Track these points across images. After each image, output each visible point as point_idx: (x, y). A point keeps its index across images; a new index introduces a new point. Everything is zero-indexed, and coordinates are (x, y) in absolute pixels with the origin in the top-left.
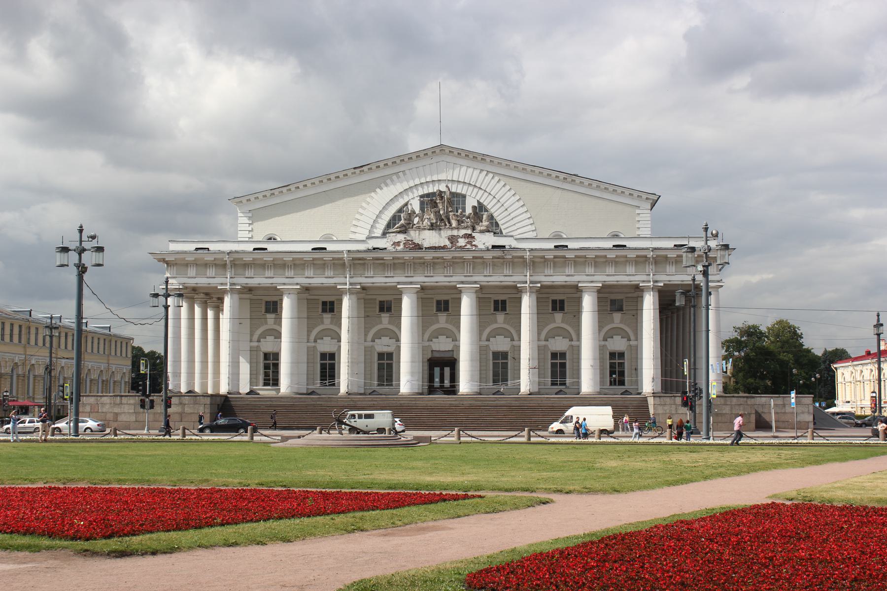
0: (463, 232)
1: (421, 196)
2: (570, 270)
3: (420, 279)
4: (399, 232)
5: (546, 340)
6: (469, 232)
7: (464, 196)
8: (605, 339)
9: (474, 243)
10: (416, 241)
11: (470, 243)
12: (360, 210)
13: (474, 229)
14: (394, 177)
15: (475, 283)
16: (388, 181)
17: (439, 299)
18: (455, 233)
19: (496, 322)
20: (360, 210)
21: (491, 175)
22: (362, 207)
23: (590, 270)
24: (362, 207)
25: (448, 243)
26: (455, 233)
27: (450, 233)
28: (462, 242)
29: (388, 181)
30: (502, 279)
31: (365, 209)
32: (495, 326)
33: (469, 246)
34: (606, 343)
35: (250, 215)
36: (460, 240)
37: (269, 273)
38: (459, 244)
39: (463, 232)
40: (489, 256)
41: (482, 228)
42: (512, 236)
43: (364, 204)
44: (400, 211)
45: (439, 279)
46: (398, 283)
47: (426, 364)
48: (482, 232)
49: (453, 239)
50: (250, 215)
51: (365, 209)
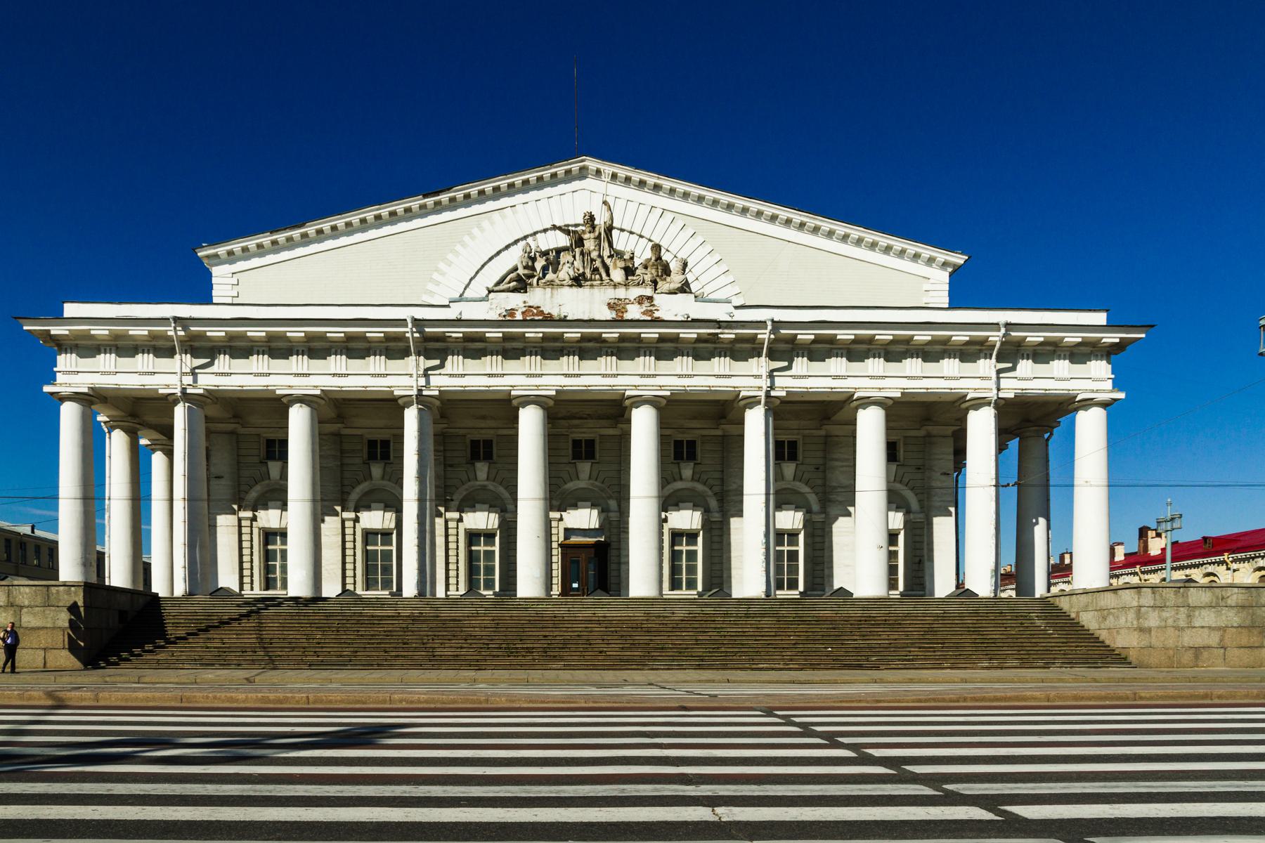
6: (648, 291)
9: (657, 314)
12: (436, 276)
15: (661, 387)
17: (577, 436)
18: (621, 293)
19: (681, 479)
20: (436, 276)
22: (437, 270)
24: (437, 270)
31: (443, 274)
32: (679, 485)
36: (628, 307)
38: (628, 316)
39: (635, 292)
40: (690, 334)
43: (442, 266)
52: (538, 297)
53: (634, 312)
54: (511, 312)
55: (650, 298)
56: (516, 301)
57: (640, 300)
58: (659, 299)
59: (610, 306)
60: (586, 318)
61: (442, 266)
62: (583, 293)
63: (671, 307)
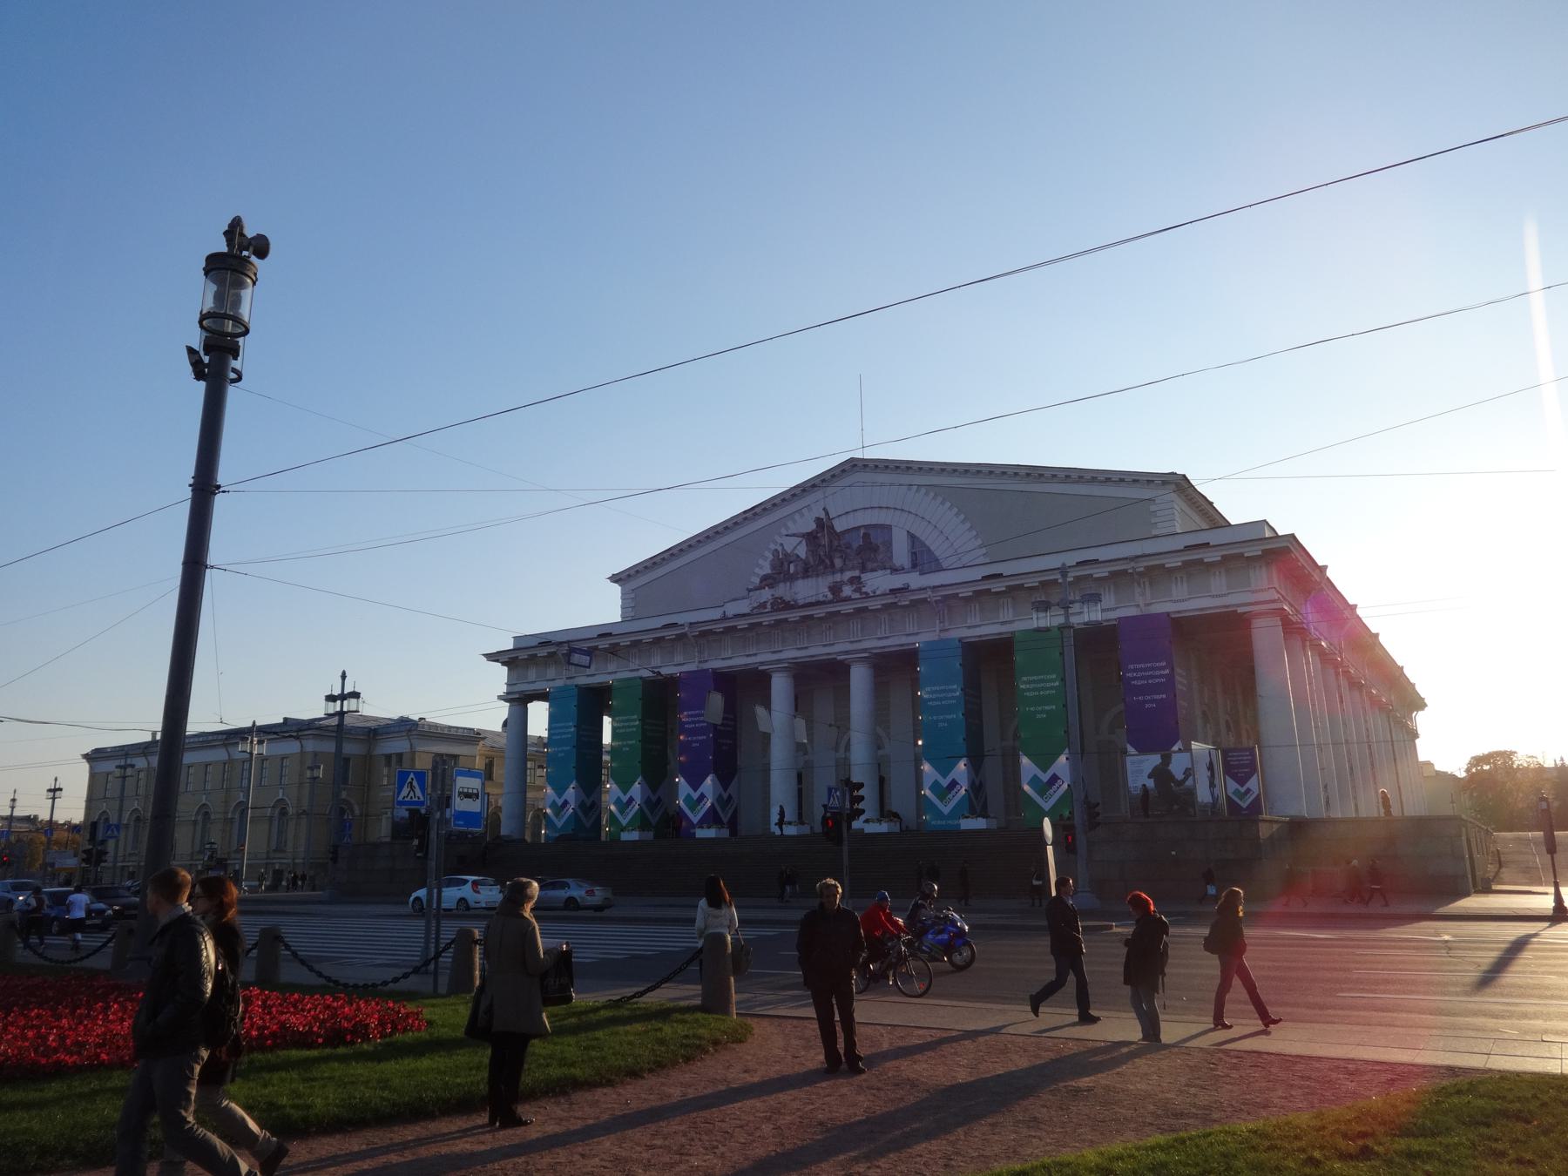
0: (848, 575)
2: (1007, 614)
3: (790, 654)
6: (856, 573)
7: (889, 528)
10: (787, 598)
11: (858, 590)
14: (797, 517)
15: (865, 650)
18: (838, 577)
21: (923, 490)
26: (838, 577)
27: (830, 579)
28: (847, 591)
33: (857, 595)
37: (611, 667)
39: (848, 575)
45: (817, 649)
46: (762, 663)
49: (835, 589)
52: (782, 590)
53: (847, 591)
54: (763, 605)
56: (766, 595)
57: (853, 580)
58: (864, 577)
60: (813, 600)
62: (811, 582)
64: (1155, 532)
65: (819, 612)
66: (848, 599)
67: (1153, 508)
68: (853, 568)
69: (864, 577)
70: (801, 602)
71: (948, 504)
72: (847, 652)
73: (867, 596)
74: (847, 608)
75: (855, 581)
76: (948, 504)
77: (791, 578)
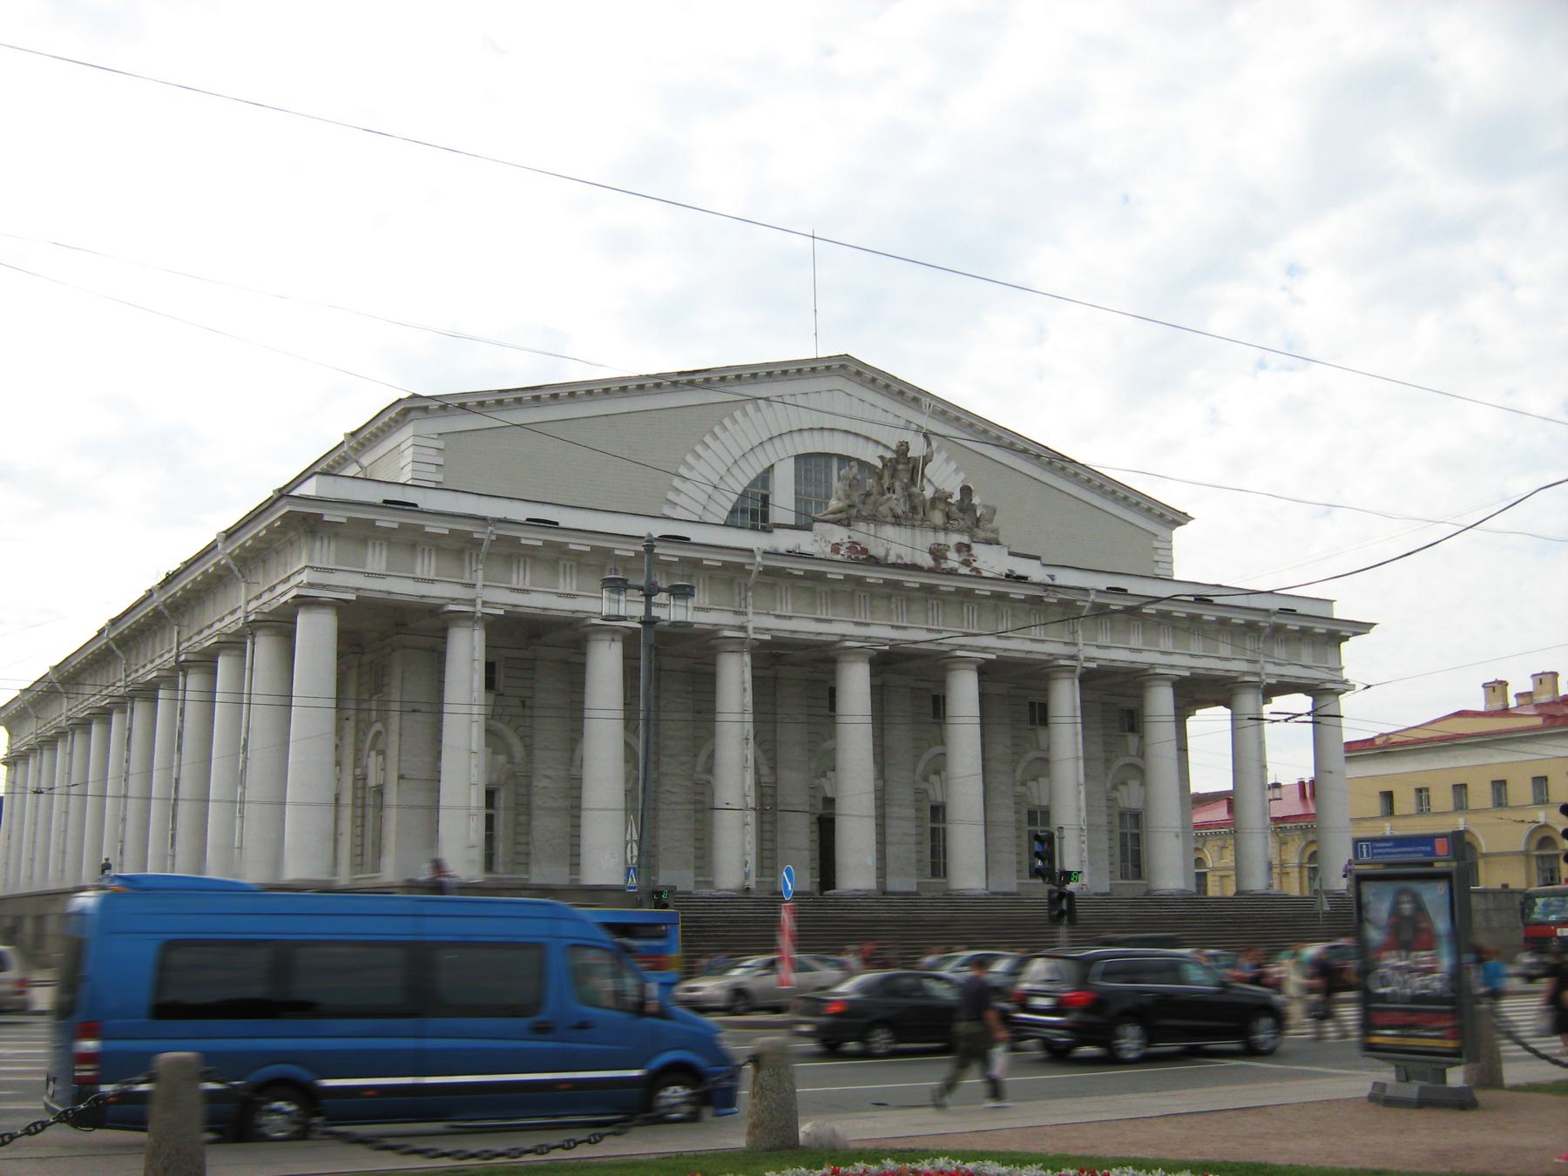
1: (798, 458)
4: (837, 522)
5: (1024, 783)
6: (965, 539)
8: (1115, 788)
11: (966, 563)
13: (972, 537)
14: (750, 407)
15: (984, 649)
16: (738, 414)
18: (941, 538)
23: (1166, 643)
25: (927, 561)
28: (953, 560)
29: (738, 414)
30: (1029, 646)
33: (964, 570)
34: (1118, 795)
35: (441, 444)
37: (565, 585)
39: (955, 539)
41: (990, 535)
42: (1038, 558)
43: (690, 458)
44: (753, 484)
47: (816, 828)
48: (988, 542)
49: (938, 553)
50: (441, 444)
51: (691, 468)
52: (862, 533)
53: (953, 560)
54: (836, 548)
55: (968, 547)
57: (961, 548)
58: (978, 549)
59: (931, 552)
61: (690, 458)
63: (992, 561)
64: (1158, 571)
65: (912, 580)
66: (952, 572)
67: (1156, 544)
68: (960, 531)
69: (978, 549)
70: (892, 559)
71: (953, 465)
72: (962, 647)
73: (977, 575)
74: (947, 584)
75: (961, 548)
76: (953, 465)
77: (873, 518)
